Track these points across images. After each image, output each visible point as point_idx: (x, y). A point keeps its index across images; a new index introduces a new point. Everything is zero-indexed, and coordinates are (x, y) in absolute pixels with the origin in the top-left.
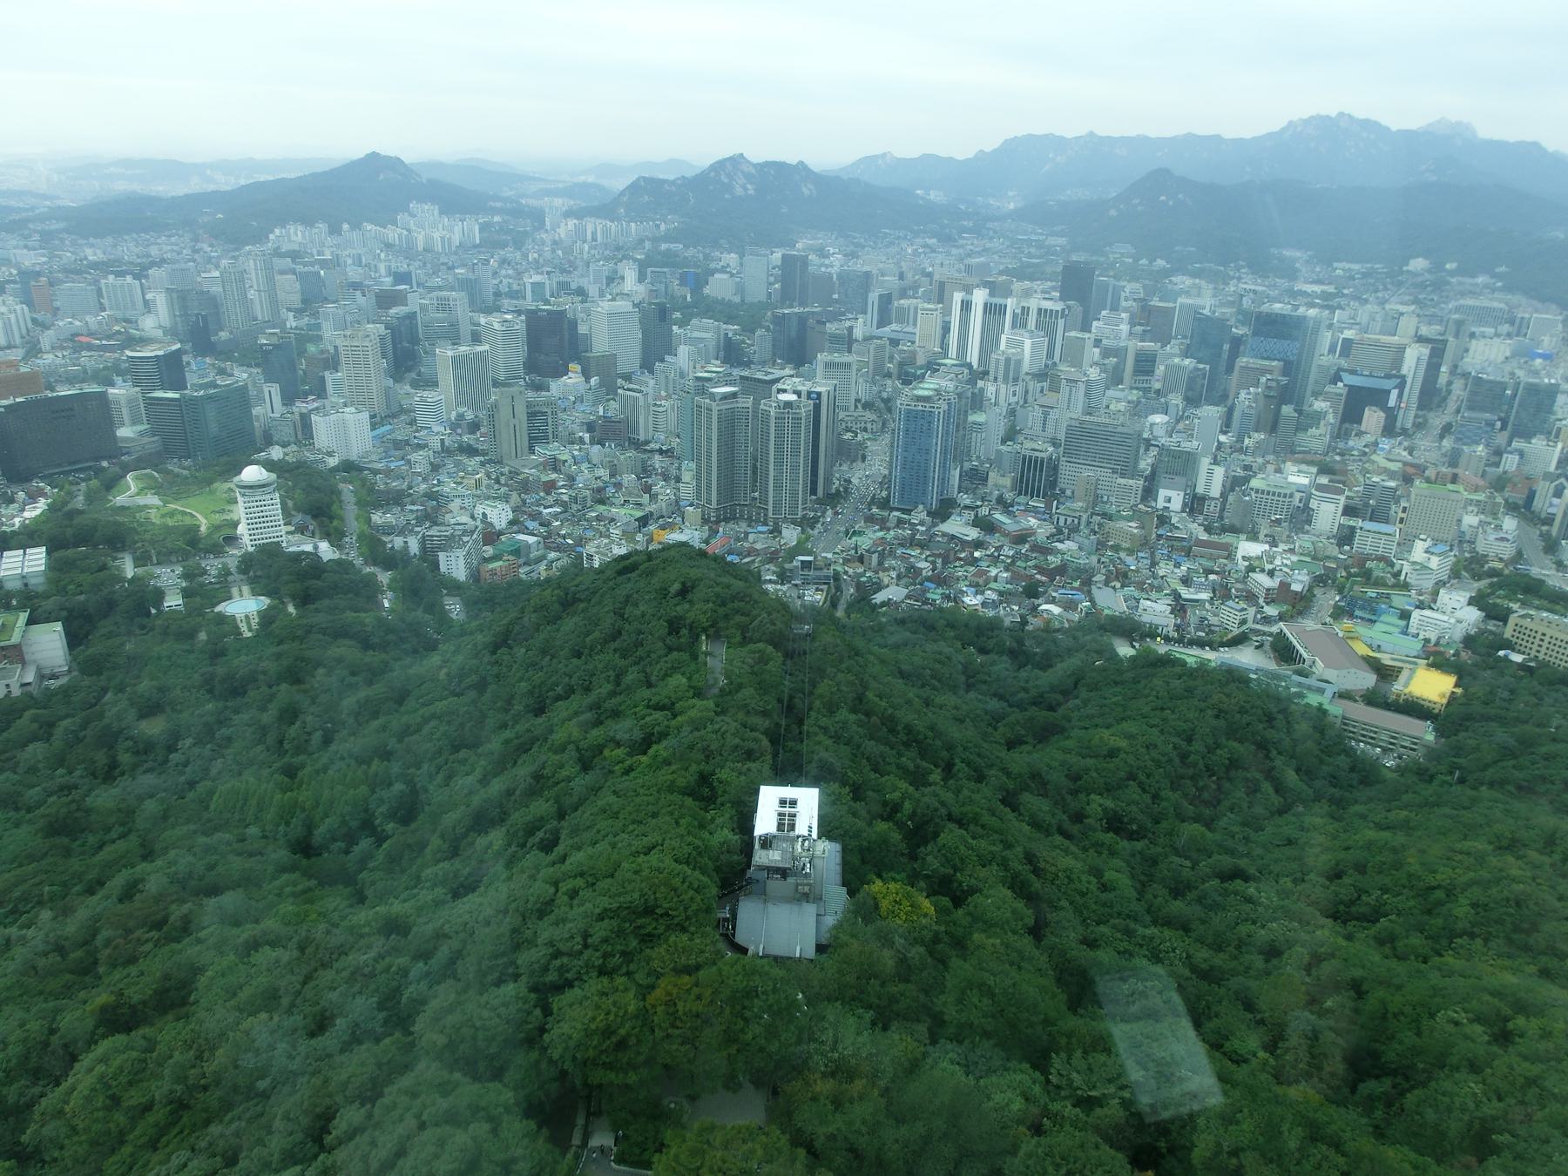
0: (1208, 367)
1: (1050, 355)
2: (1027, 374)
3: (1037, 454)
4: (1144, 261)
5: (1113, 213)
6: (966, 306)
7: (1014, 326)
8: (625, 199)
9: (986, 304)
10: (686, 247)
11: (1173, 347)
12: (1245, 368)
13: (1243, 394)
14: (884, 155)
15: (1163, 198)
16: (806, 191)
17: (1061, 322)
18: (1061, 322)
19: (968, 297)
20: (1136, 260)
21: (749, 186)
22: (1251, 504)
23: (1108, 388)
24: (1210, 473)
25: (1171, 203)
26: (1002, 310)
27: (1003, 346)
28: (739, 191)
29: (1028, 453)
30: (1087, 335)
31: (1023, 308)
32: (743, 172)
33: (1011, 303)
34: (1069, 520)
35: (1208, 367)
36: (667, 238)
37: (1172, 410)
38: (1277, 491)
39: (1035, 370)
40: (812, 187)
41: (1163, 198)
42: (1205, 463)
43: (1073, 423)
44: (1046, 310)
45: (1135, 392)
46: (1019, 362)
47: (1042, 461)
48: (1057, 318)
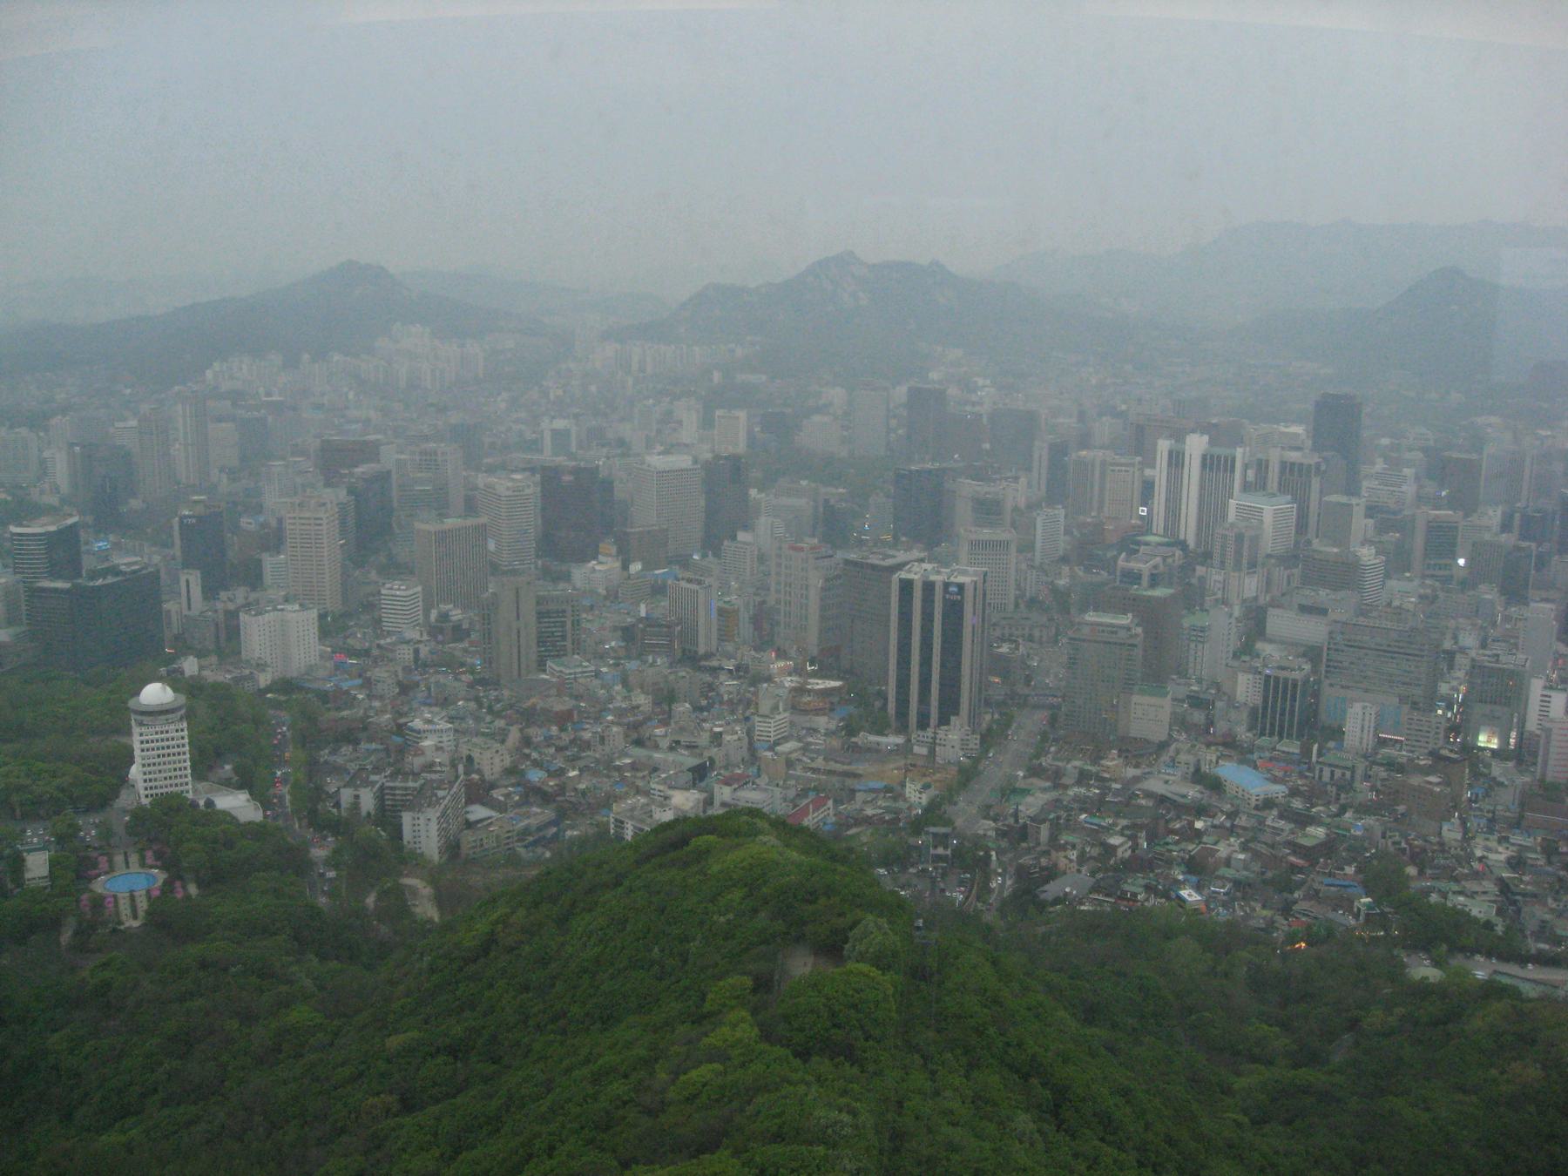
1: (1302, 526)
2: (1269, 556)
6: (1176, 460)
7: (1246, 487)
9: (1204, 457)
17: (1316, 483)
23: (1387, 576)
24: (1545, 700)
27: (1232, 515)
30: (1354, 501)
34: (1338, 773)
42: (1536, 687)
44: (1293, 464)
47: (1295, 686)
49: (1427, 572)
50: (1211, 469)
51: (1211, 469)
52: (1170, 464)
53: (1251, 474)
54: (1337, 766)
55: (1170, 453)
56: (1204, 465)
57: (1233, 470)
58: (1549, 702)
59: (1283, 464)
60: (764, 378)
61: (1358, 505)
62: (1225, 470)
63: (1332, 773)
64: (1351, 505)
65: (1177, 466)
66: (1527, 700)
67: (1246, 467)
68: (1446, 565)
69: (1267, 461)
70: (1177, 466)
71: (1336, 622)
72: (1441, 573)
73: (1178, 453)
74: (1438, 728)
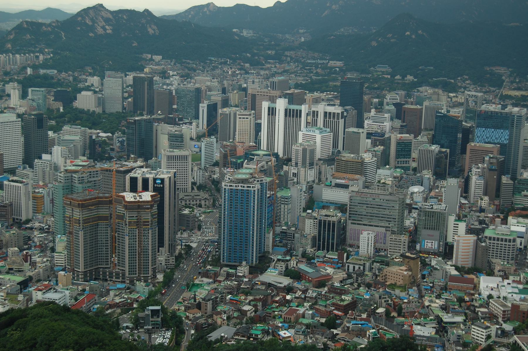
0: (448, 150)
1: (335, 144)
2: (320, 160)
3: (329, 219)
4: (398, 77)
5: (374, 44)
6: (272, 112)
8: (12, 37)
9: (286, 110)
10: (60, 71)
11: (423, 138)
12: (473, 150)
13: (474, 170)
14: (208, 5)
15: (408, 33)
16: (151, 31)
18: (342, 121)
19: (272, 105)
20: (393, 76)
21: (107, 27)
22: (486, 249)
23: (378, 168)
24: (456, 227)
25: (414, 37)
26: (298, 113)
27: (300, 140)
28: (100, 31)
29: (323, 218)
30: (361, 130)
31: (314, 112)
32: (102, 17)
33: (304, 108)
34: (357, 267)
35: (448, 150)
36: (45, 66)
37: (426, 182)
38: (504, 237)
39: (325, 157)
40: (155, 27)
41: (408, 33)
42: (452, 219)
43: (354, 194)
44: (330, 113)
45: (398, 170)
46: (313, 152)
48: (338, 119)
49: (397, 165)
50: (290, 116)
51: (290, 116)
52: (269, 114)
53: (310, 118)
54: (356, 264)
55: (269, 108)
56: (286, 115)
57: (300, 116)
58: (458, 227)
59: (325, 113)
60: (56, 71)
61: (363, 132)
62: (297, 117)
63: (354, 267)
64: (359, 133)
65: (272, 114)
66: (447, 226)
67: (308, 115)
68: (406, 161)
69: (317, 112)
70: (272, 114)
71: (353, 191)
72: (405, 165)
73: (273, 108)
74: (404, 242)
